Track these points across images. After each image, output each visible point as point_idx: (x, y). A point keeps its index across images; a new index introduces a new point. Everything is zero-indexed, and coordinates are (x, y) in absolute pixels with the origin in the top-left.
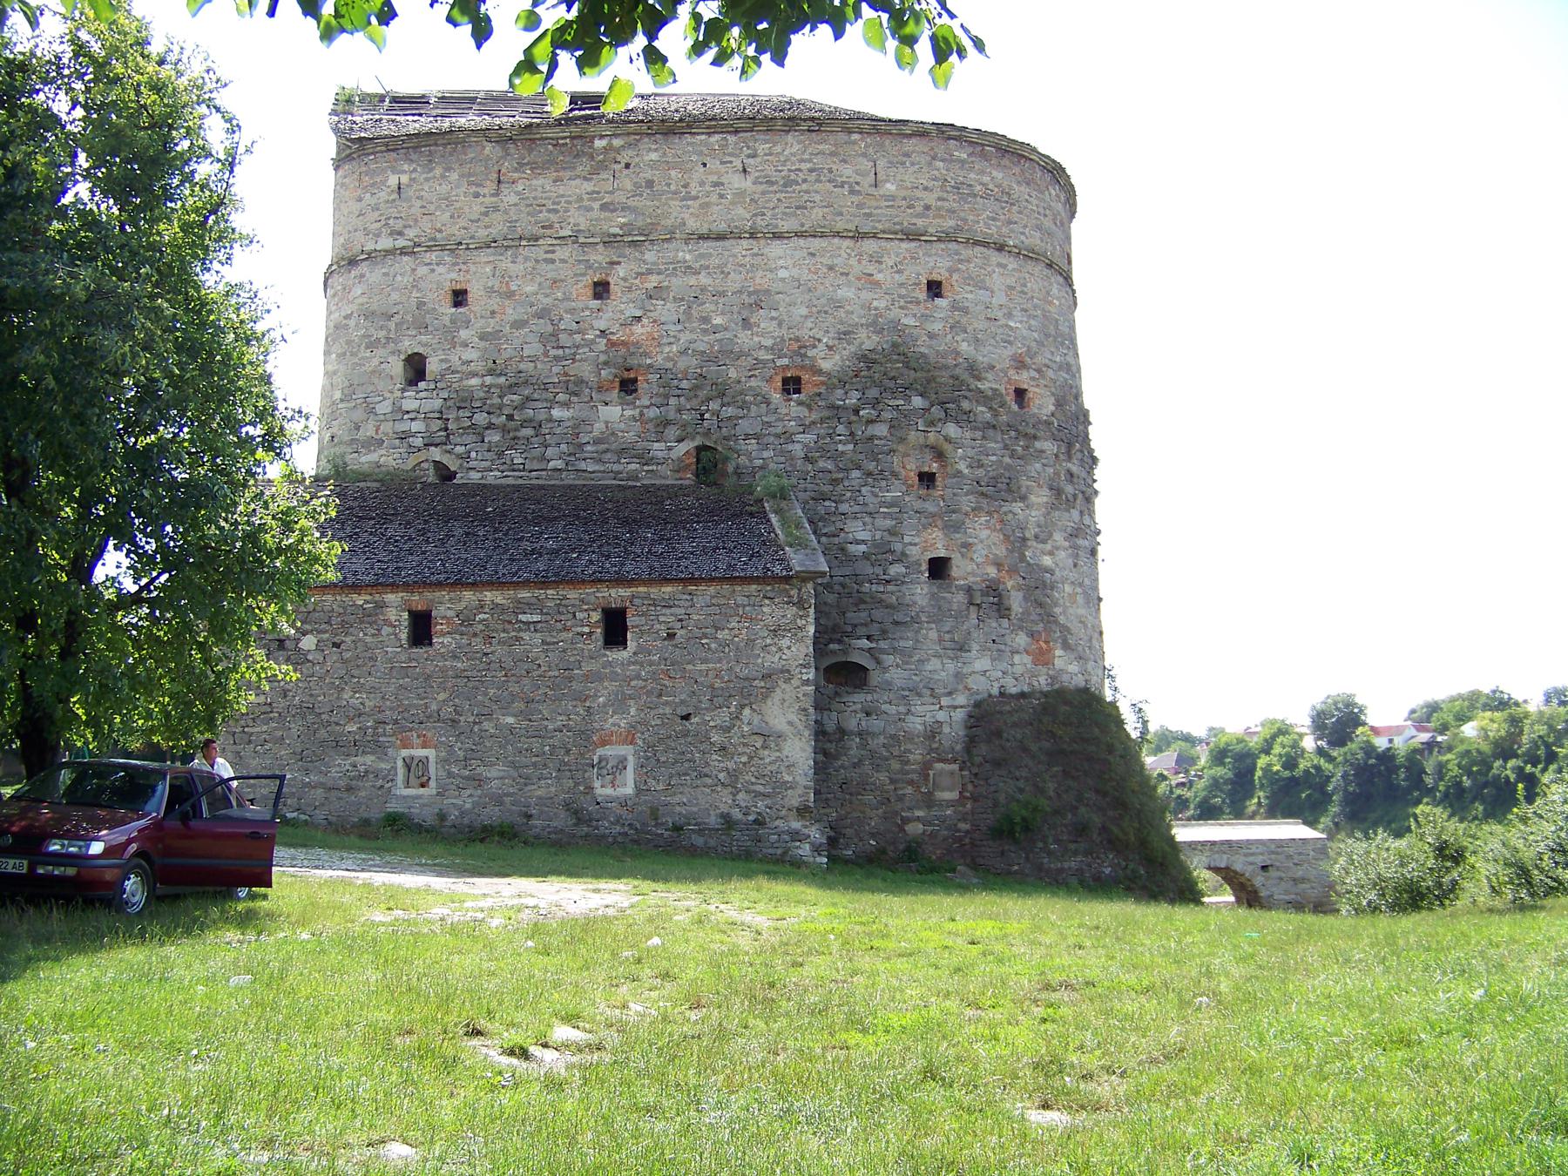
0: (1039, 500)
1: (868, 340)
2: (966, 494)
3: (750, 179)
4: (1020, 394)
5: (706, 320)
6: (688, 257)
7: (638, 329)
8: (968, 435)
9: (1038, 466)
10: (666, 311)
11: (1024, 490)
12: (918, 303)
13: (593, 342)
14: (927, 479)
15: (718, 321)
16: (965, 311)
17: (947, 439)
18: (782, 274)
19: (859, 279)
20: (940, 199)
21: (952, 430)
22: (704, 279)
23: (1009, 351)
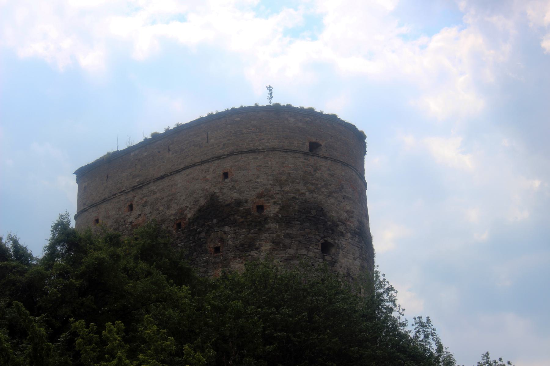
0: (266, 248)
1: (202, 202)
2: (231, 252)
3: (171, 153)
4: (260, 208)
5: (158, 209)
6: (154, 188)
7: (140, 219)
8: (232, 229)
9: (266, 234)
10: (147, 210)
11: (257, 246)
12: (220, 182)
13: (128, 227)
14: (217, 250)
15: (161, 208)
16: (236, 181)
17: (225, 233)
18: (179, 185)
19: (201, 180)
20: (228, 140)
21: (227, 229)
22: (158, 195)
23: (254, 193)
